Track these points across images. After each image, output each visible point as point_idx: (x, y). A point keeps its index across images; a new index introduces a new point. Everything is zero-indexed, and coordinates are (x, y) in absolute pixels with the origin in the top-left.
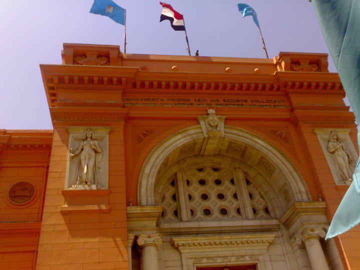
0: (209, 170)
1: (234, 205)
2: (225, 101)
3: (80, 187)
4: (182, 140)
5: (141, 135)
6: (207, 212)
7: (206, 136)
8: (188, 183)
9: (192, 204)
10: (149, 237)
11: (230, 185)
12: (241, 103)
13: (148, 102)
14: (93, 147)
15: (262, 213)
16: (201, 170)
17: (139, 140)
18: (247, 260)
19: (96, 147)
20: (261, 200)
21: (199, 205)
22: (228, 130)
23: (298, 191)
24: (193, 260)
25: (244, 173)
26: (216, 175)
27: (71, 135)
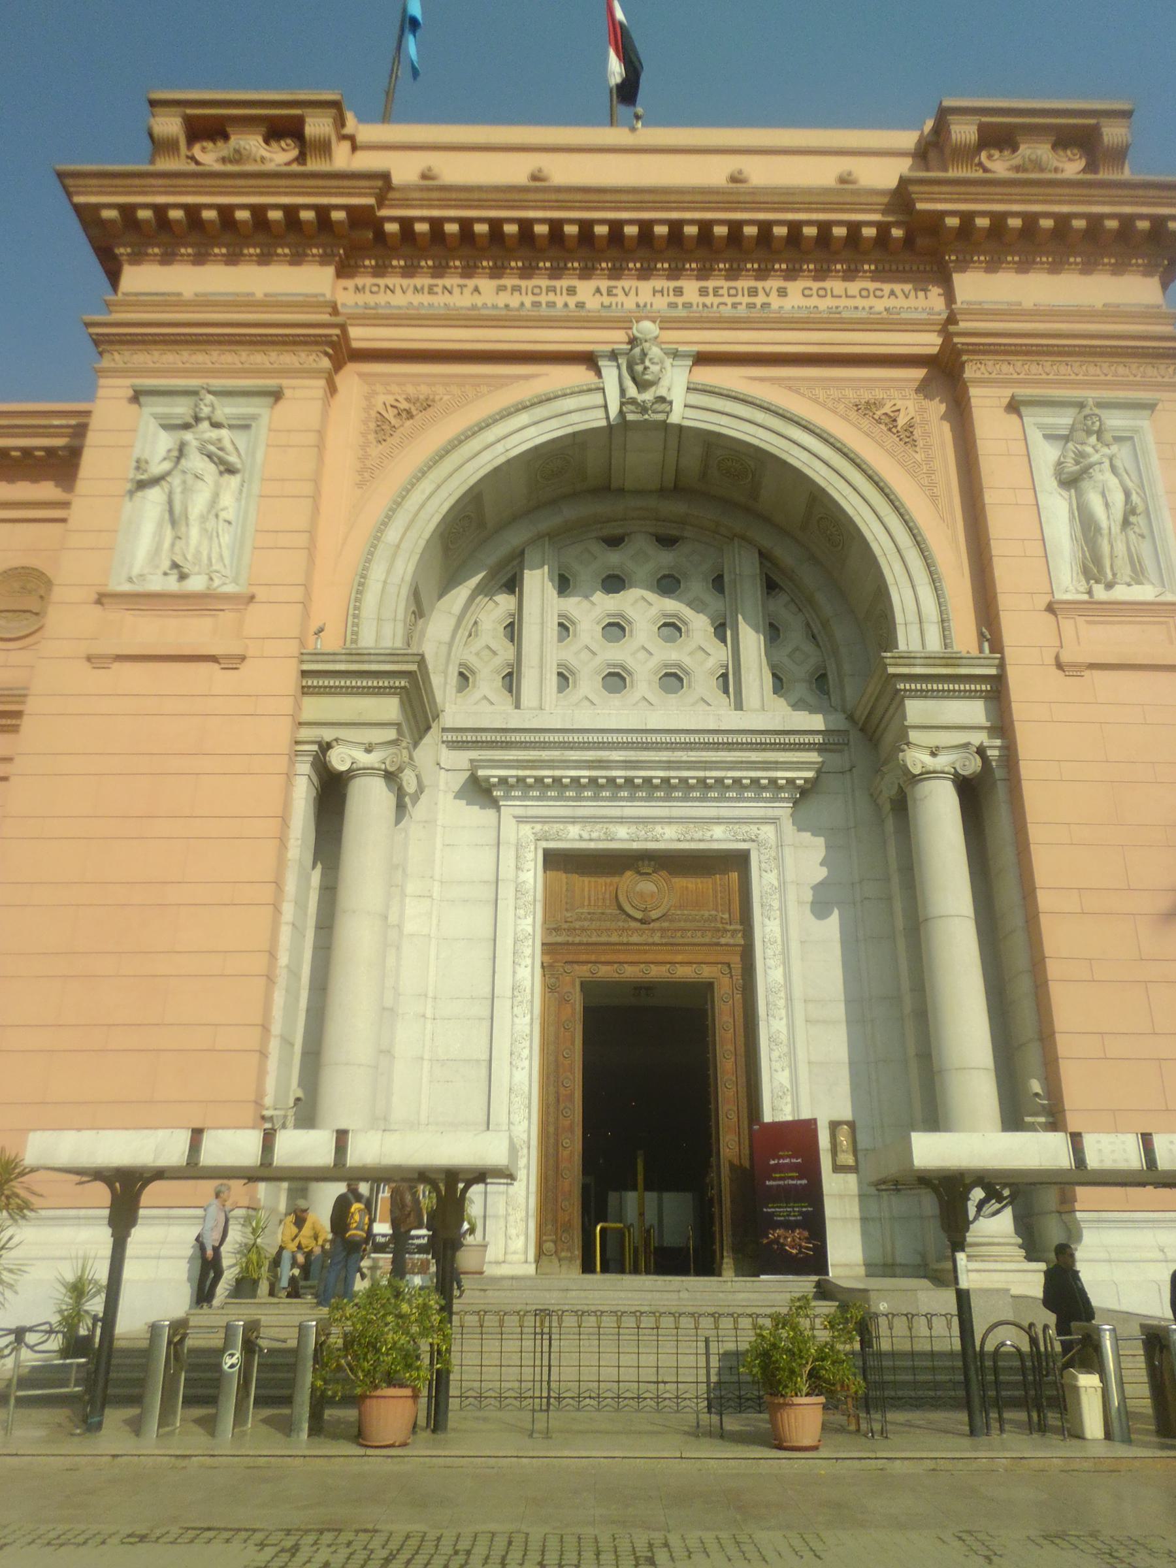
0: (641, 543)
1: (711, 662)
2: (703, 292)
3: (158, 583)
4: (532, 431)
5: (390, 415)
8: (564, 585)
10: (369, 749)
12: (760, 300)
13: (425, 299)
14: (212, 448)
15: (801, 690)
16: (614, 542)
18: (715, 837)
20: (808, 647)
21: (590, 652)
23: (912, 617)
24: (538, 827)
25: (761, 554)
27: (147, 411)
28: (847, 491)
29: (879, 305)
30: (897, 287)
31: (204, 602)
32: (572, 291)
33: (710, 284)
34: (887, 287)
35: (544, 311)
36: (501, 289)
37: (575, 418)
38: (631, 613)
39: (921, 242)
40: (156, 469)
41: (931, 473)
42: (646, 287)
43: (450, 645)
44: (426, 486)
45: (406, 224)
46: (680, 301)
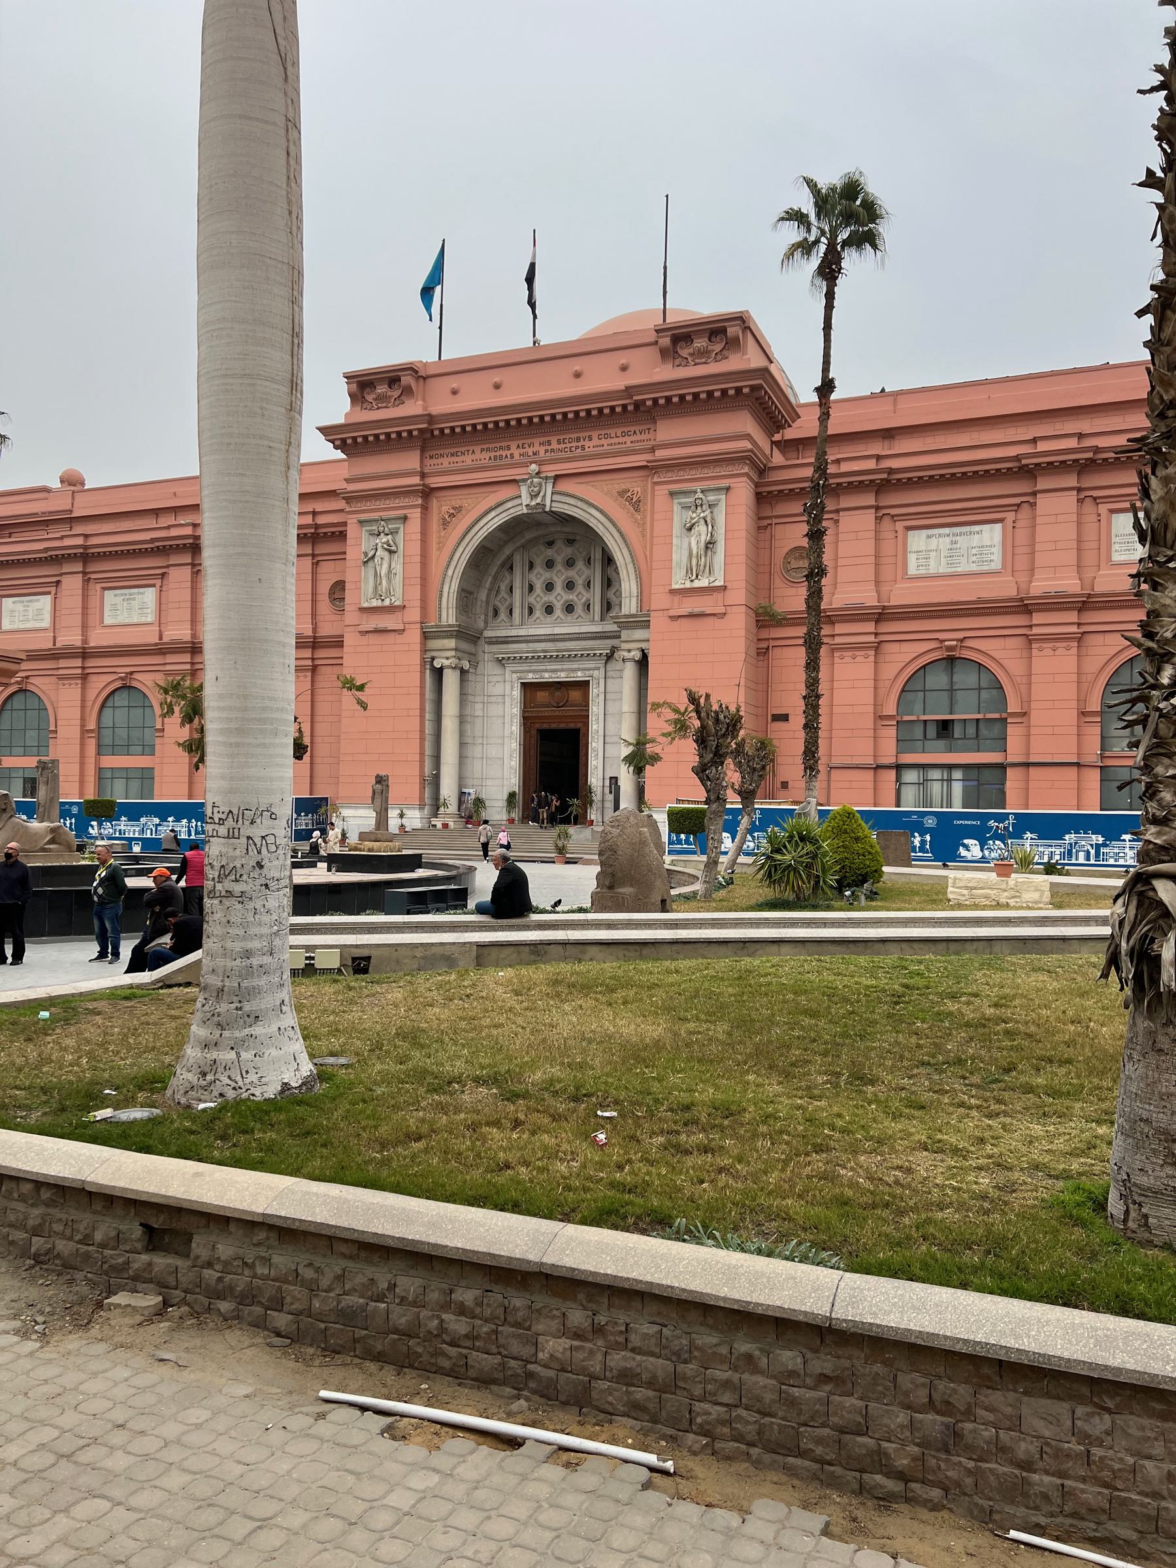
0: (559, 544)
2: (559, 442)
3: (375, 603)
4: (496, 519)
6: (549, 610)
7: (525, 511)
9: (531, 599)
10: (447, 658)
11: (584, 569)
12: (579, 444)
13: (455, 459)
16: (550, 544)
17: (445, 524)
19: (389, 545)
21: (539, 598)
22: (556, 497)
26: (568, 551)
28: (610, 538)
29: (628, 439)
30: (637, 428)
31: (392, 609)
32: (509, 448)
33: (561, 437)
34: (632, 429)
35: (498, 462)
36: (482, 450)
37: (512, 511)
38: (555, 578)
39: (642, 409)
40: (371, 554)
41: (644, 524)
42: (536, 441)
43: (487, 602)
44: (461, 549)
45: (442, 430)
46: (549, 448)
